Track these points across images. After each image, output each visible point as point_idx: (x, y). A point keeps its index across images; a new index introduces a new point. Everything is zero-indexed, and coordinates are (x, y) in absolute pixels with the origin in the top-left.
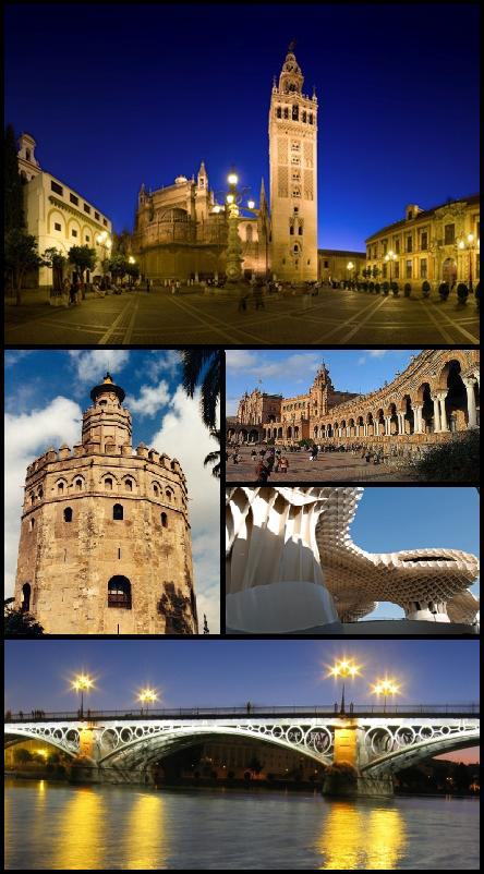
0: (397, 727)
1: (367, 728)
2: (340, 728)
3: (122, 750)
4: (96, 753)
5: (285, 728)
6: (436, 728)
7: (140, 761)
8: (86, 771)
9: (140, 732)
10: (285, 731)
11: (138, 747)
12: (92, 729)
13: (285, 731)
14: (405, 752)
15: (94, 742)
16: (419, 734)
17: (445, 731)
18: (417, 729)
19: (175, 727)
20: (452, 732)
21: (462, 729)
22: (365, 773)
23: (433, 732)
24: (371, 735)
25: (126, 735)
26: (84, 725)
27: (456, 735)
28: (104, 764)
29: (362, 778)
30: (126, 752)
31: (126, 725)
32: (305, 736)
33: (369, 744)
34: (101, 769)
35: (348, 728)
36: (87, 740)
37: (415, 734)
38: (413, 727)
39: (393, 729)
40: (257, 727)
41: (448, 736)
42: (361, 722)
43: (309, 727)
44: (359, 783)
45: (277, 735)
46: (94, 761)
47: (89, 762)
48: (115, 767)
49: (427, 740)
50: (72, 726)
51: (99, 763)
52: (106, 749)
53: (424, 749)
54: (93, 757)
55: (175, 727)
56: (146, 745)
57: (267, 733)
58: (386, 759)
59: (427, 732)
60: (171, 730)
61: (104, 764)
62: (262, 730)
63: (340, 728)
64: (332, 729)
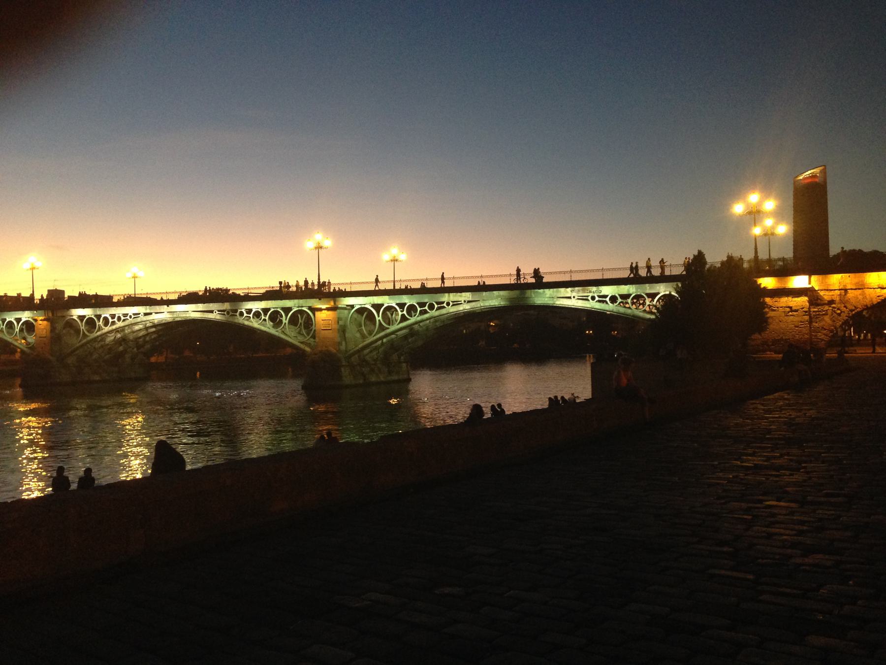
0: (383, 305)
2: (320, 310)
5: (266, 311)
6: (422, 305)
10: (265, 315)
13: (265, 315)
17: (431, 307)
19: (146, 314)
20: (439, 309)
21: (448, 304)
23: (419, 309)
27: (443, 311)
32: (285, 320)
35: (328, 309)
43: (290, 309)
55: (146, 314)
60: (142, 318)
63: (320, 310)
64: (314, 310)
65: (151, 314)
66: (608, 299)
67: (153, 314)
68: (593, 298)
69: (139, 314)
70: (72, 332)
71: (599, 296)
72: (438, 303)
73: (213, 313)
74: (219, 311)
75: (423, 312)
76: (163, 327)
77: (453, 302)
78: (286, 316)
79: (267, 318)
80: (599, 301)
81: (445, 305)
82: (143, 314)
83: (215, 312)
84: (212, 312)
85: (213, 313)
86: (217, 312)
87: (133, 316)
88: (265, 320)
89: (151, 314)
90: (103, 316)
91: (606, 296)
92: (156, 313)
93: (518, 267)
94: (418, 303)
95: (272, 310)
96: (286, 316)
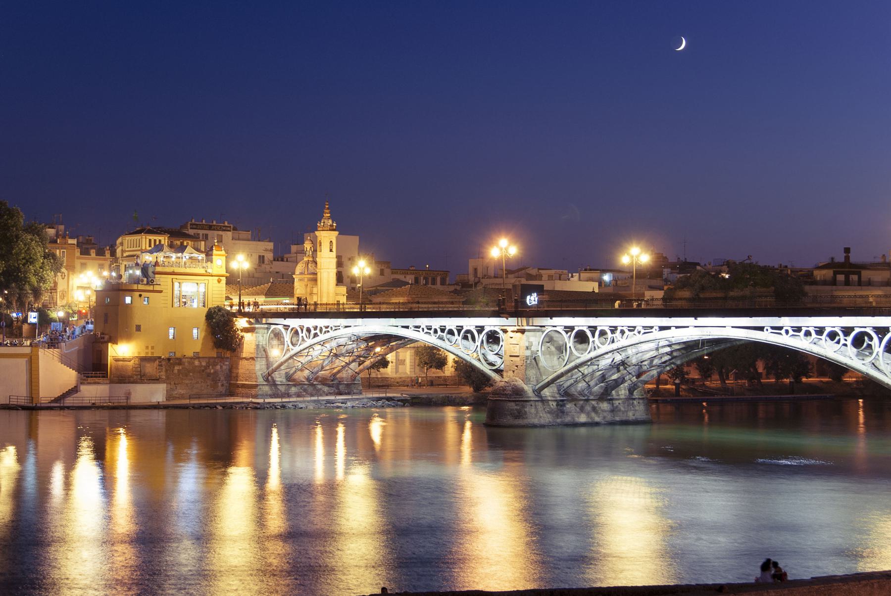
3: (577, 367)
4: (532, 373)
5: (847, 331)
7: (617, 383)
8: (512, 406)
9: (603, 333)
11: (605, 362)
12: (523, 332)
15: (528, 353)
19: (662, 328)
25: (581, 338)
26: (511, 323)
28: (546, 392)
30: (585, 370)
31: (581, 323)
34: (543, 401)
36: (516, 351)
46: (528, 389)
47: (518, 392)
48: (567, 396)
50: (491, 323)
51: (538, 392)
52: (552, 366)
54: (526, 380)
55: (662, 328)
56: (618, 358)
61: (546, 392)
65: (668, 328)
67: (672, 328)
69: (652, 327)
70: (553, 349)
73: (763, 331)
74: (773, 328)
76: (683, 346)
78: (881, 340)
79: (849, 342)
82: (657, 328)
83: (767, 330)
84: (761, 329)
85: (763, 331)
86: (770, 330)
87: (643, 331)
88: (845, 345)
89: (668, 328)
90: (599, 329)
92: (677, 327)
95: (857, 330)
96: (881, 340)
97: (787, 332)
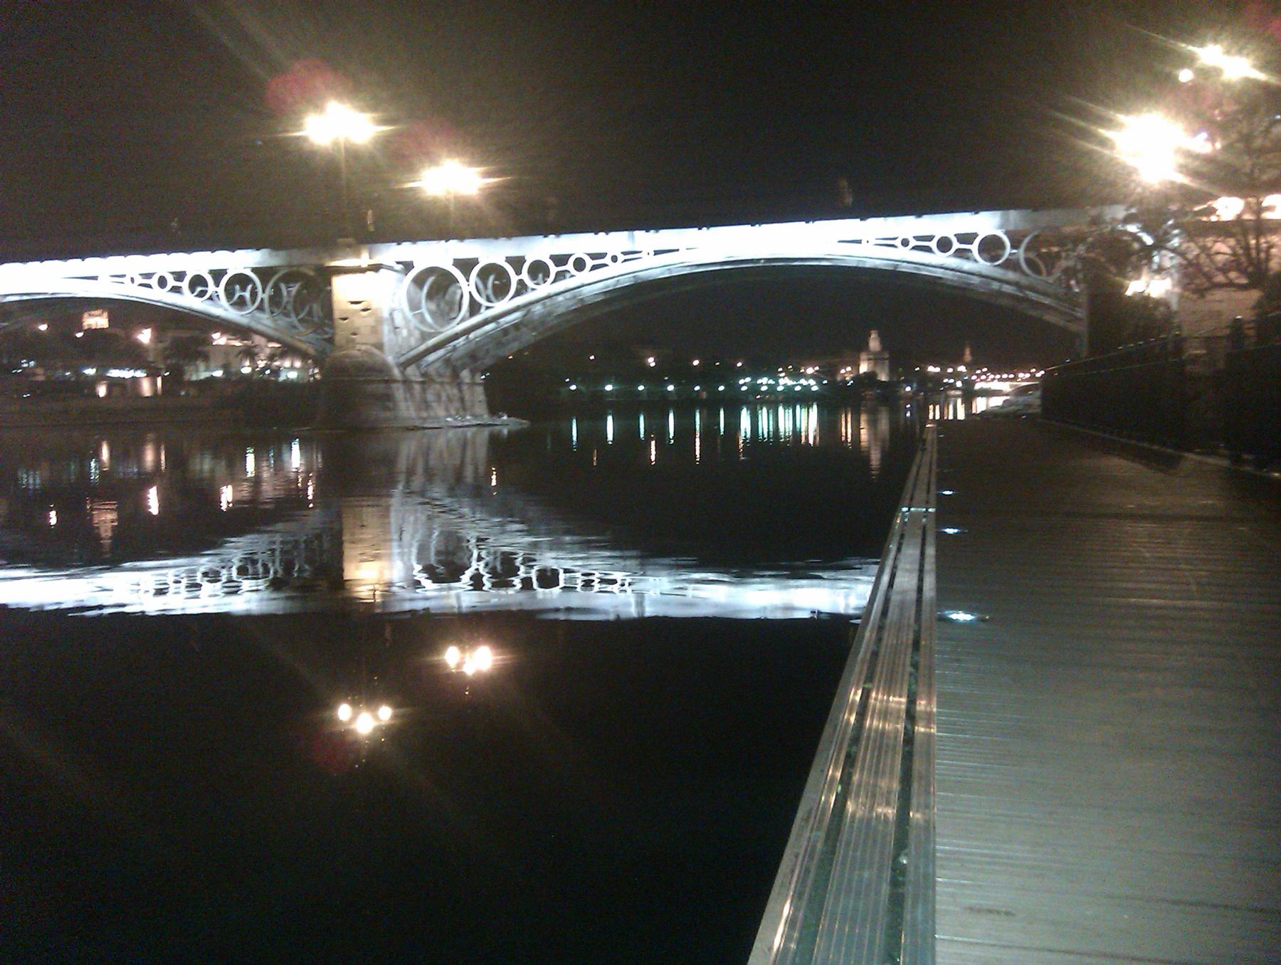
0: (474, 262)
1: (408, 266)
5: (218, 275)
6: (560, 260)
14: (495, 319)
16: (525, 276)
17: (580, 265)
18: (517, 262)
20: (594, 268)
22: (411, 371)
23: (554, 270)
24: (419, 281)
29: (407, 382)
33: (414, 306)
37: (514, 279)
38: (509, 260)
39: (466, 265)
40: (149, 276)
41: (585, 276)
42: (391, 253)
44: (399, 392)
45: (202, 294)
49: (545, 289)
53: (538, 308)
57: (176, 290)
58: (456, 336)
59: (538, 270)
62: (162, 282)
66: (933, 244)
68: (905, 243)
71: (917, 238)
72: (594, 256)
75: (560, 276)
77: (625, 253)
80: (915, 248)
81: (607, 260)
91: (930, 238)
93: (914, 237)
94: (552, 257)
97: (132, 280)
